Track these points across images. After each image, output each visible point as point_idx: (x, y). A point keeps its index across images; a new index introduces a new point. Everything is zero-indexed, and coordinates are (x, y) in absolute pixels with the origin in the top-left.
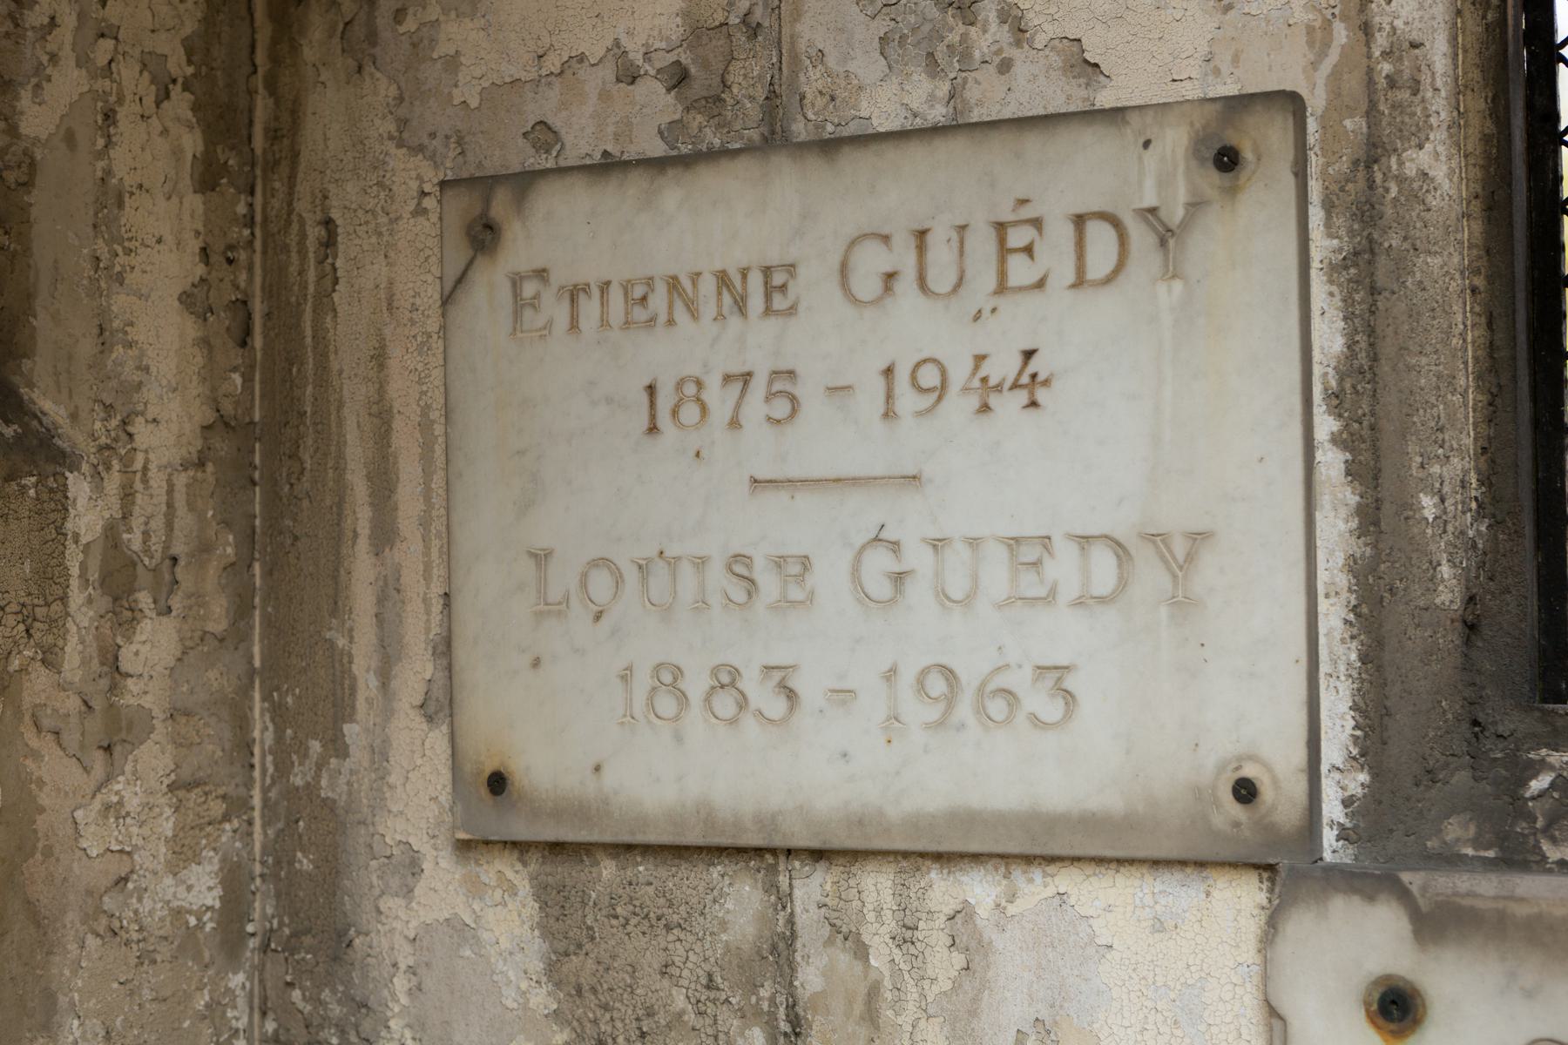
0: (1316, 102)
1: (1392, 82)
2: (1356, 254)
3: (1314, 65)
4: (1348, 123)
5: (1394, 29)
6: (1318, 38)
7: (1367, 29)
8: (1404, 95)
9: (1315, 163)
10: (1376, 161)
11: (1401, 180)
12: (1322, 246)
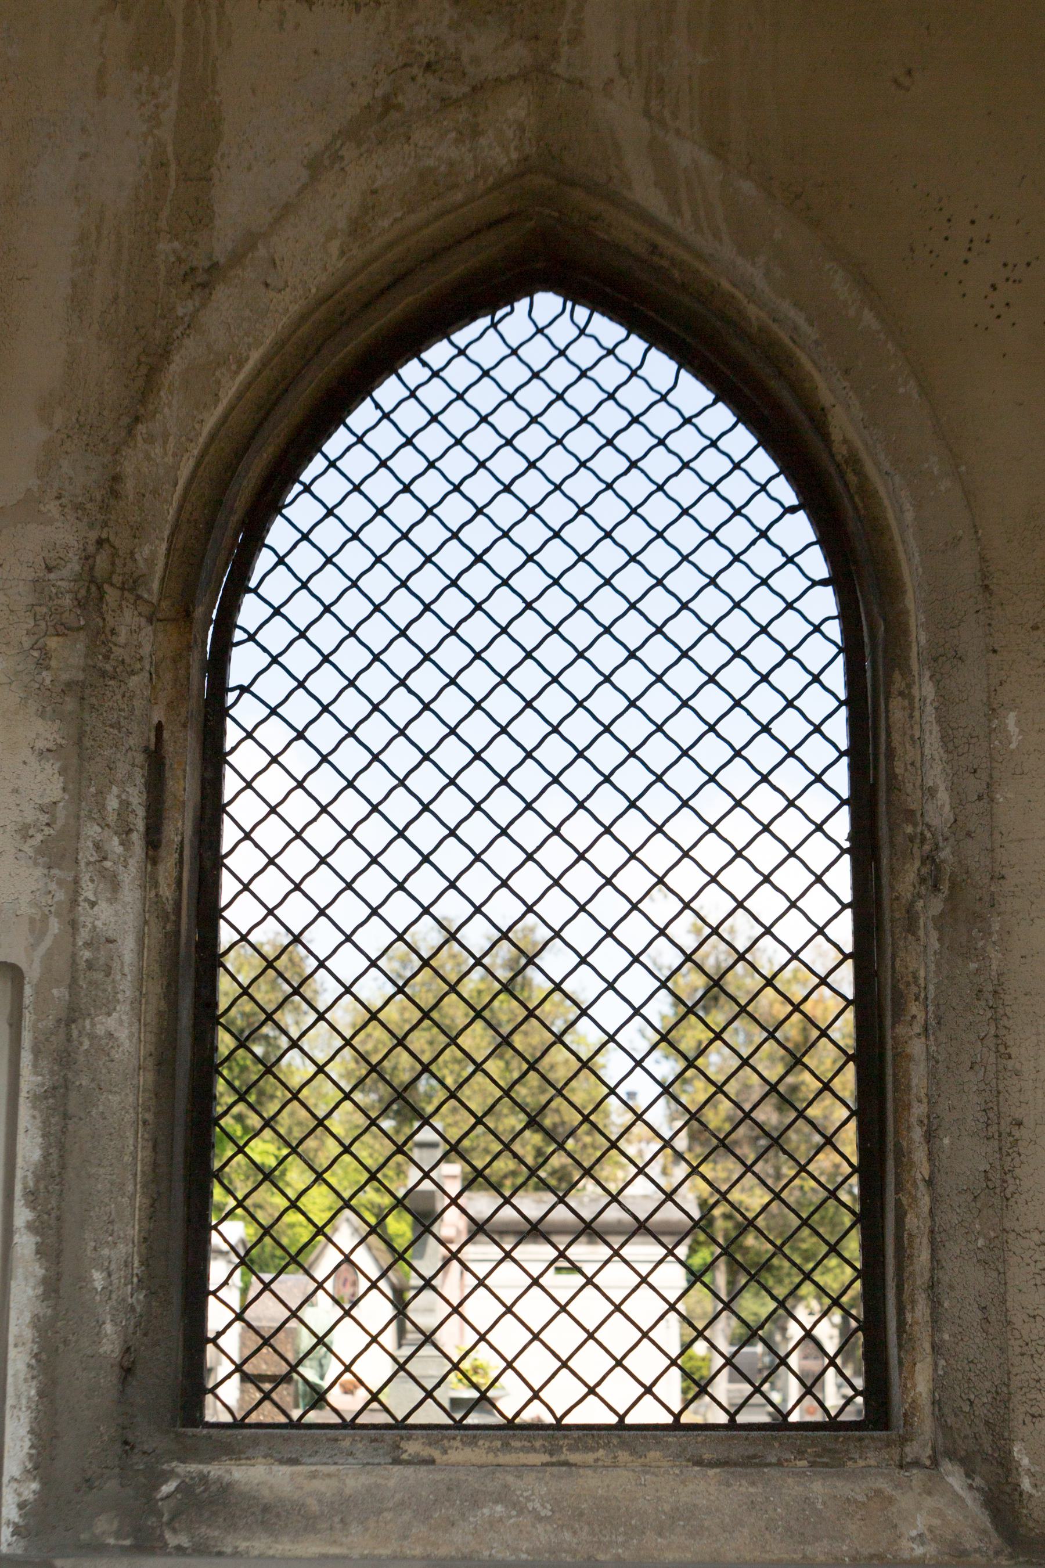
0: (33, 973)
1: (90, 965)
2: (54, 1088)
3: (33, 946)
4: (55, 991)
5: (94, 927)
6: (37, 928)
7: (74, 925)
8: (99, 976)
9: (28, 1018)
10: (74, 1021)
11: (92, 1037)
12: (29, 1081)
